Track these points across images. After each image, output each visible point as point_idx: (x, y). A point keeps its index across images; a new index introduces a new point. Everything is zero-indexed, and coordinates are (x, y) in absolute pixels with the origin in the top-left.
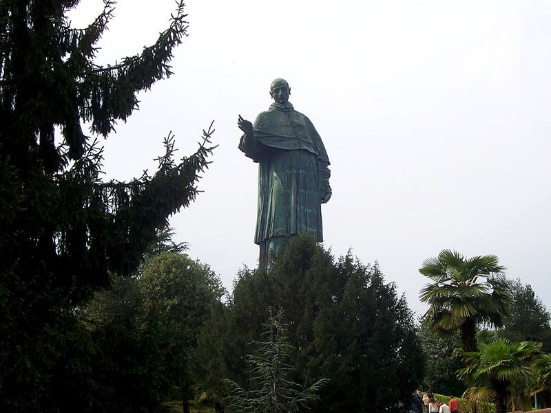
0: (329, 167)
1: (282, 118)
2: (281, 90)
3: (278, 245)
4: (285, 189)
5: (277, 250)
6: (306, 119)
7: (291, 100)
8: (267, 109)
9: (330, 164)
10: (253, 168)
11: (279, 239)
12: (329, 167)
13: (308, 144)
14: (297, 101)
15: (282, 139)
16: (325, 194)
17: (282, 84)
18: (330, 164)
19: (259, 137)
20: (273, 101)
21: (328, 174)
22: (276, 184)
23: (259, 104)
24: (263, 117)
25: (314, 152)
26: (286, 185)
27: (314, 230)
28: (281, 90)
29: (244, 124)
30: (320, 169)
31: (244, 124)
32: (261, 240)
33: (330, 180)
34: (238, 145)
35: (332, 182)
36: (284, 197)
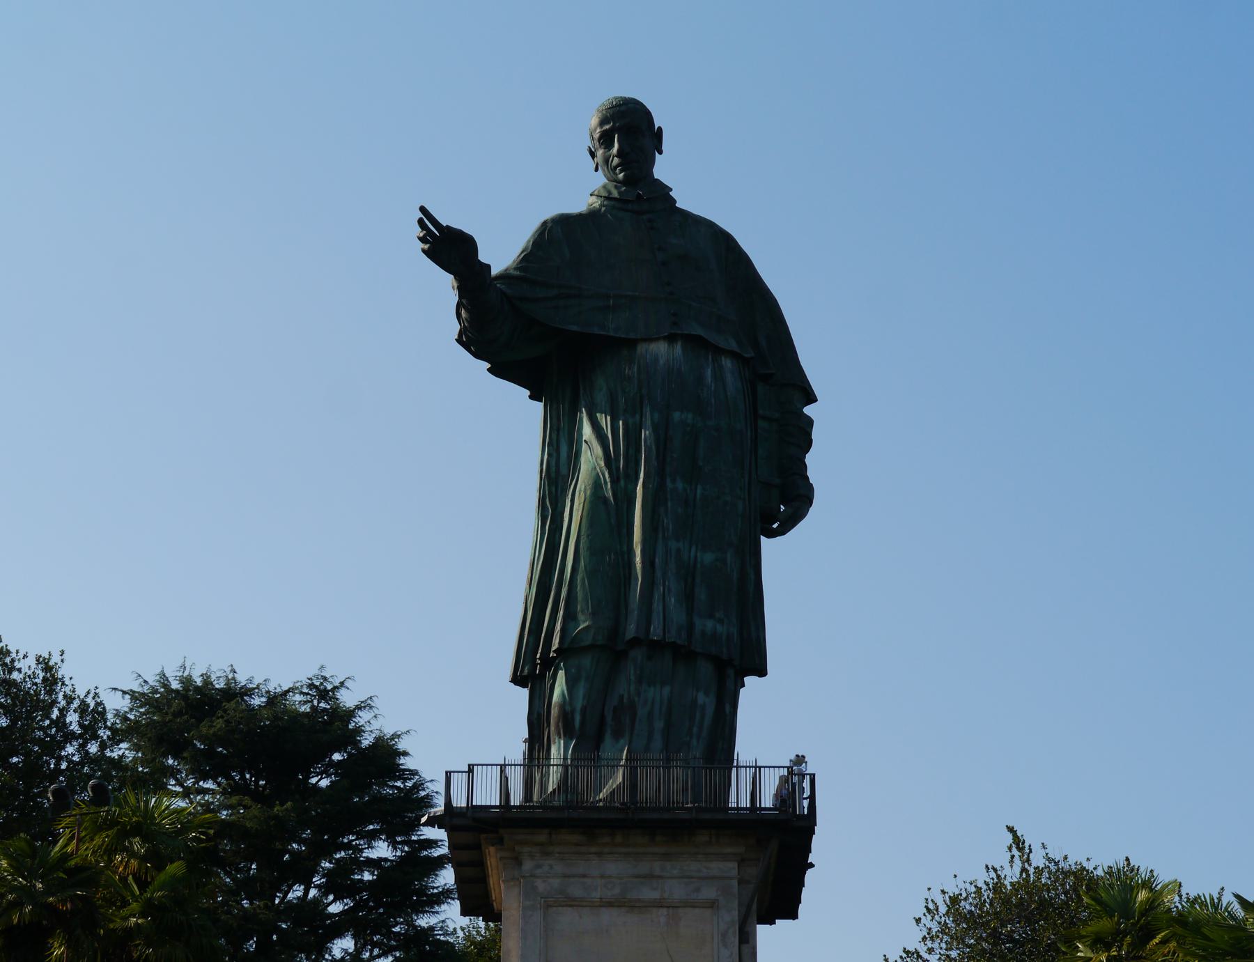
0: (808, 410)
3: (582, 683)
4: (615, 481)
5: (579, 704)
7: (662, 169)
9: (811, 398)
10: (518, 414)
11: (587, 661)
12: (808, 410)
16: (788, 499)
18: (811, 398)
21: (802, 435)
22: (591, 458)
24: (558, 236)
25: (733, 345)
26: (620, 469)
27: (719, 628)
28: (629, 133)
29: (448, 247)
30: (761, 412)
31: (448, 247)
33: (810, 459)
35: (815, 463)
36: (609, 514)
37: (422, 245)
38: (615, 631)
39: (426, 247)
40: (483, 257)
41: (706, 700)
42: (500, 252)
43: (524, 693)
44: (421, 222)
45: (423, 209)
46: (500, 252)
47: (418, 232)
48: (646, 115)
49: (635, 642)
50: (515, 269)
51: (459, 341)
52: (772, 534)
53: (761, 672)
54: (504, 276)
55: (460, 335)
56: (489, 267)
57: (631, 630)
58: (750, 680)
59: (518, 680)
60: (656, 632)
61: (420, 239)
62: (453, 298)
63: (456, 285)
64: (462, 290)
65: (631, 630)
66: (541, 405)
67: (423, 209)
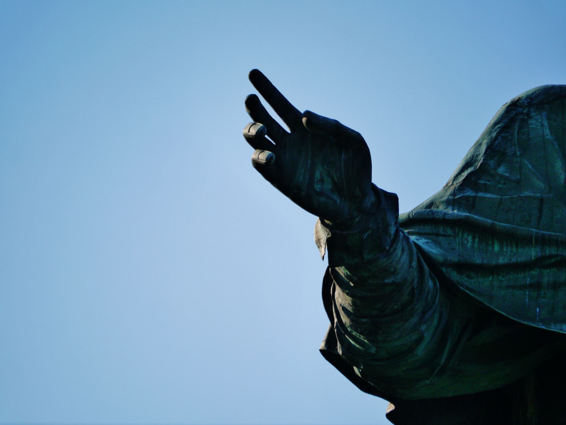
19: (464, 267)
29: (309, 156)
31: (309, 156)
34: (322, 345)
37: (251, 153)
39: (263, 156)
40: (381, 178)
42: (414, 169)
44: (252, 104)
45: (257, 78)
46: (414, 169)
47: (245, 123)
50: (449, 203)
51: (328, 353)
54: (425, 219)
55: (331, 340)
56: (393, 199)
61: (251, 140)
63: (324, 235)
64: (336, 249)
67: (257, 78)
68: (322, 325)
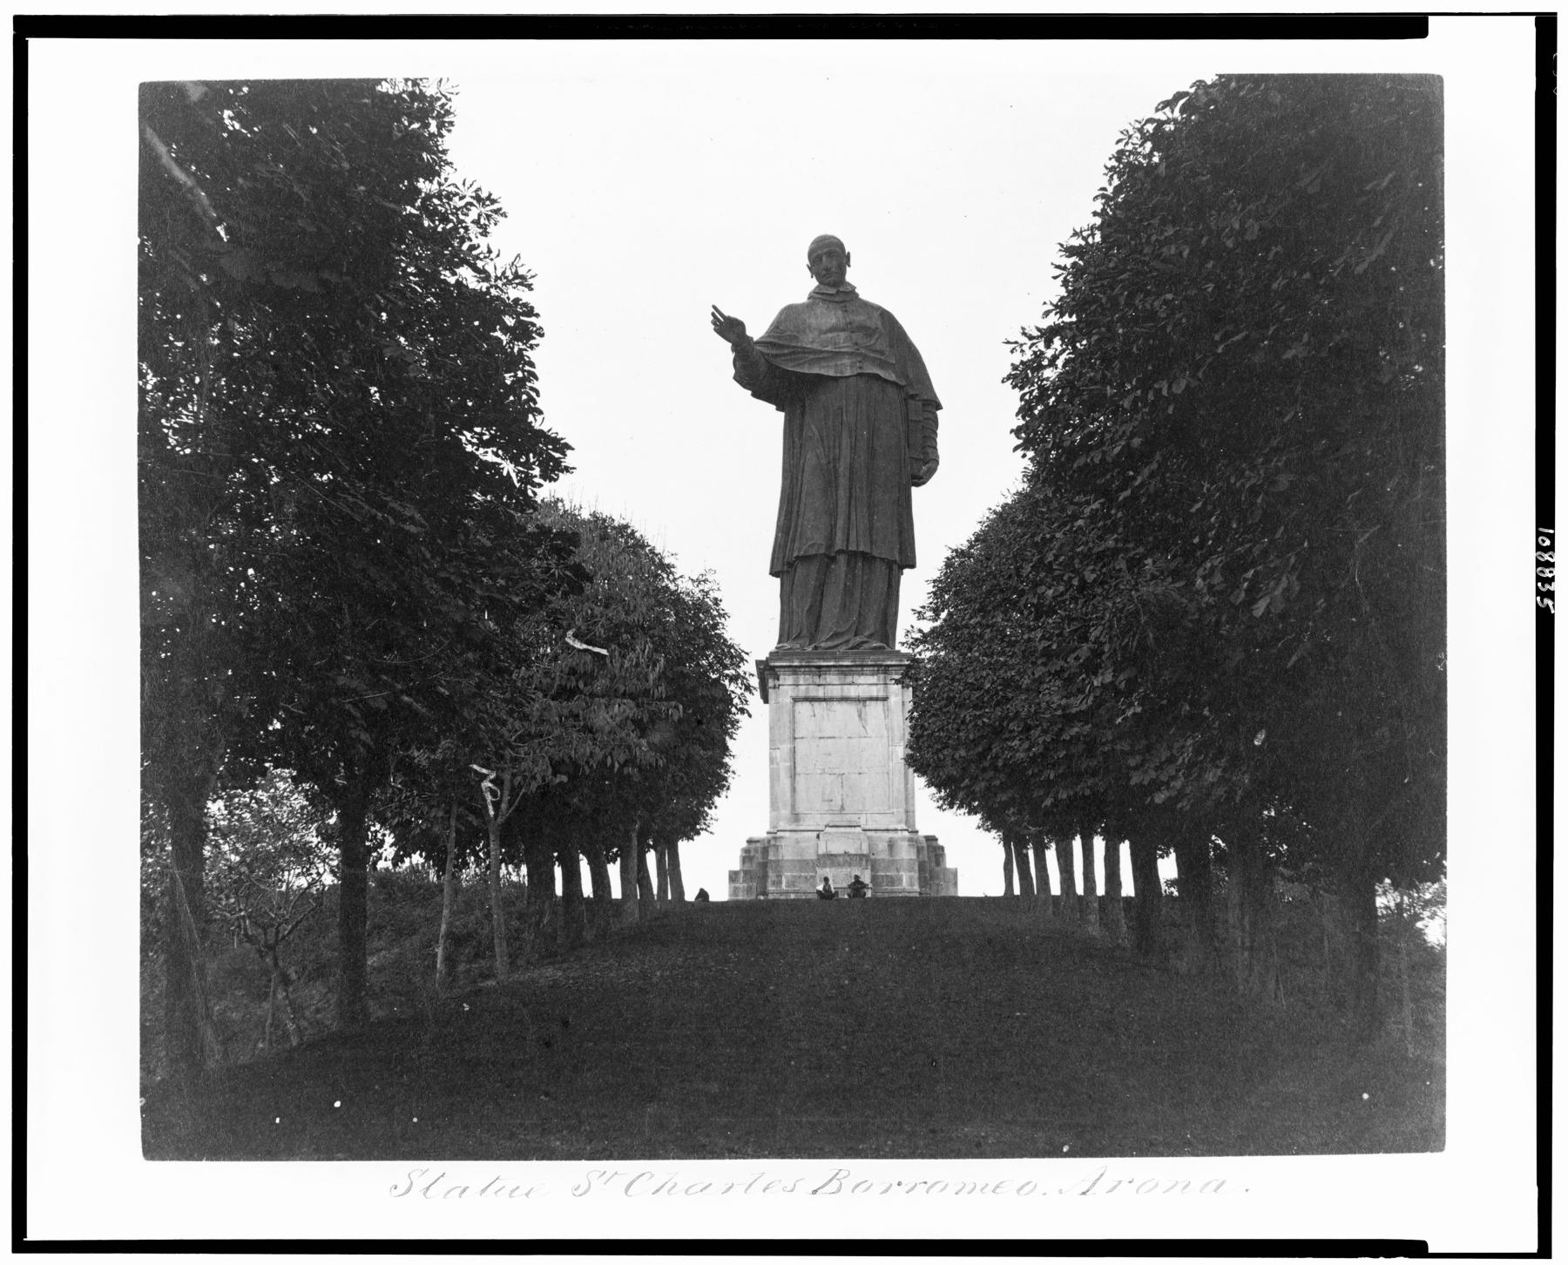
1: (830, 317)
2: (828, 259)
6: (887, 318)
7: (851, 276)
8: (801, 298)
10: (769, 420)
13: (883, 364)
14: (865, 280)
15: (820, 356)
17: (829, 245)
18: (939, 407)
20: (814, 283)
23: (772, 291)
25: (893, 377)
29: (729, 328)
31: (729, 328)
32: (784, 565)
38: (830, 546)
40: (749, 333)
41: (882, 586)
42: (756, 330)
43: (778, 581)
46: (756, 330)
48: (841, 246)
49: (840, 552)
52: (918, 485)
53: (913, 566)
54: (757, 343)
57: (839, 544)
58: (906, 571)
59: (774, 573)
60: (853, 548)
62: (732, 356)
65: (839, 544)
66: (782, 414)
68: (733, 371)
